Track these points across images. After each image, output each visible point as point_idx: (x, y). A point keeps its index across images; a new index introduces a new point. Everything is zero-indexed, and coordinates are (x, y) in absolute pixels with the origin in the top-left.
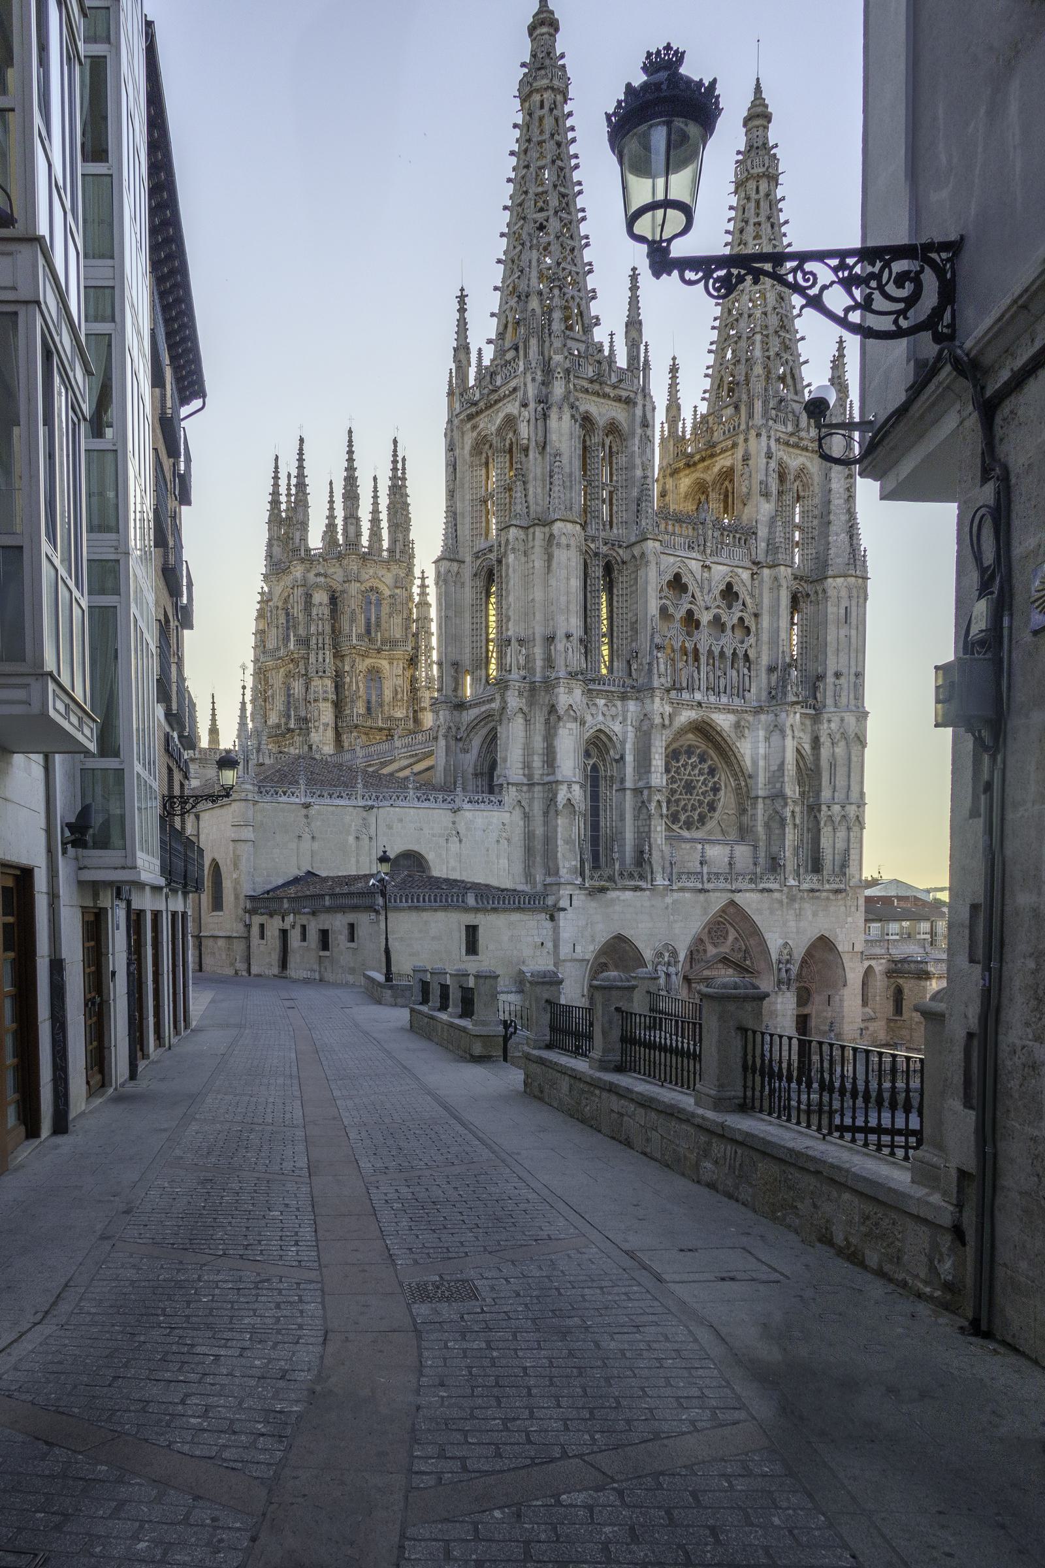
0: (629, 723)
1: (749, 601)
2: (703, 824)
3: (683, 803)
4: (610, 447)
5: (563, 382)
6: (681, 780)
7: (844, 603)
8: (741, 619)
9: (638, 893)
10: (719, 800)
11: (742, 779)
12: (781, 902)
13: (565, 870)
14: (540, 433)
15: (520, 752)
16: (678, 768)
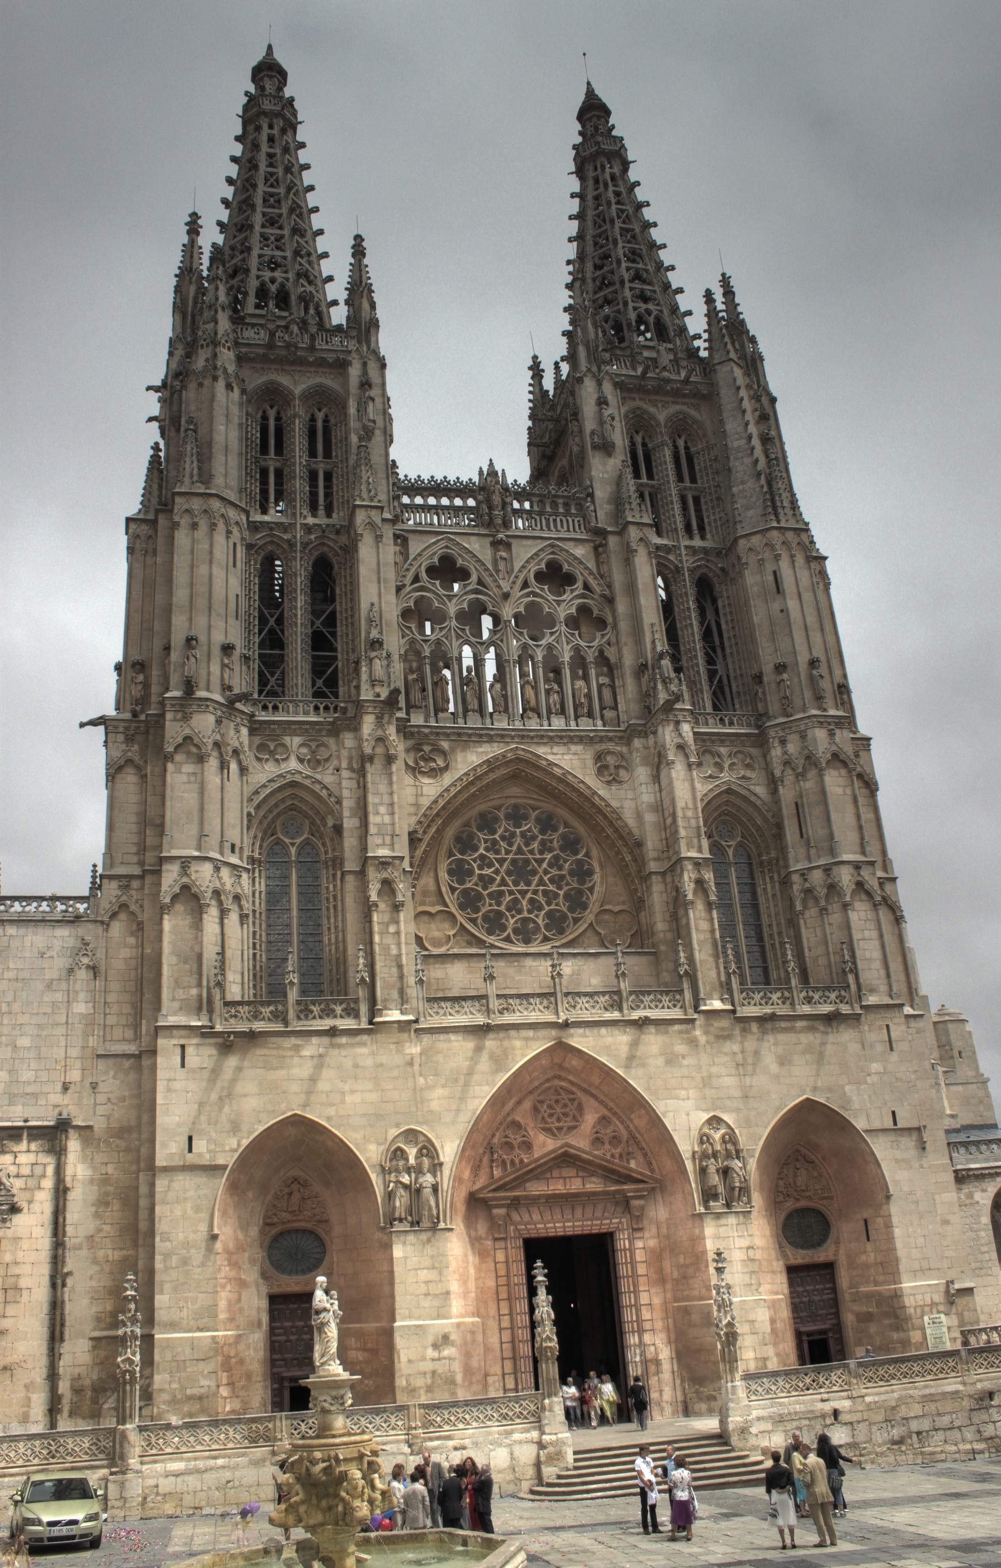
0: (344, 764)
1: (593, 583)
2: (561, 931)
3: (508, 899)
4: (326, 421)
5: (211, 347)
6: (501, 861)
7: (770, 567)
8: (584, 610)
9: (344, 1040)
10: (591, 889)
11: (624, 850)
12: (693, 1042)
13: (176, 1005)
14: (175, 408)
15: (134, 828)
16: (494, 842)
